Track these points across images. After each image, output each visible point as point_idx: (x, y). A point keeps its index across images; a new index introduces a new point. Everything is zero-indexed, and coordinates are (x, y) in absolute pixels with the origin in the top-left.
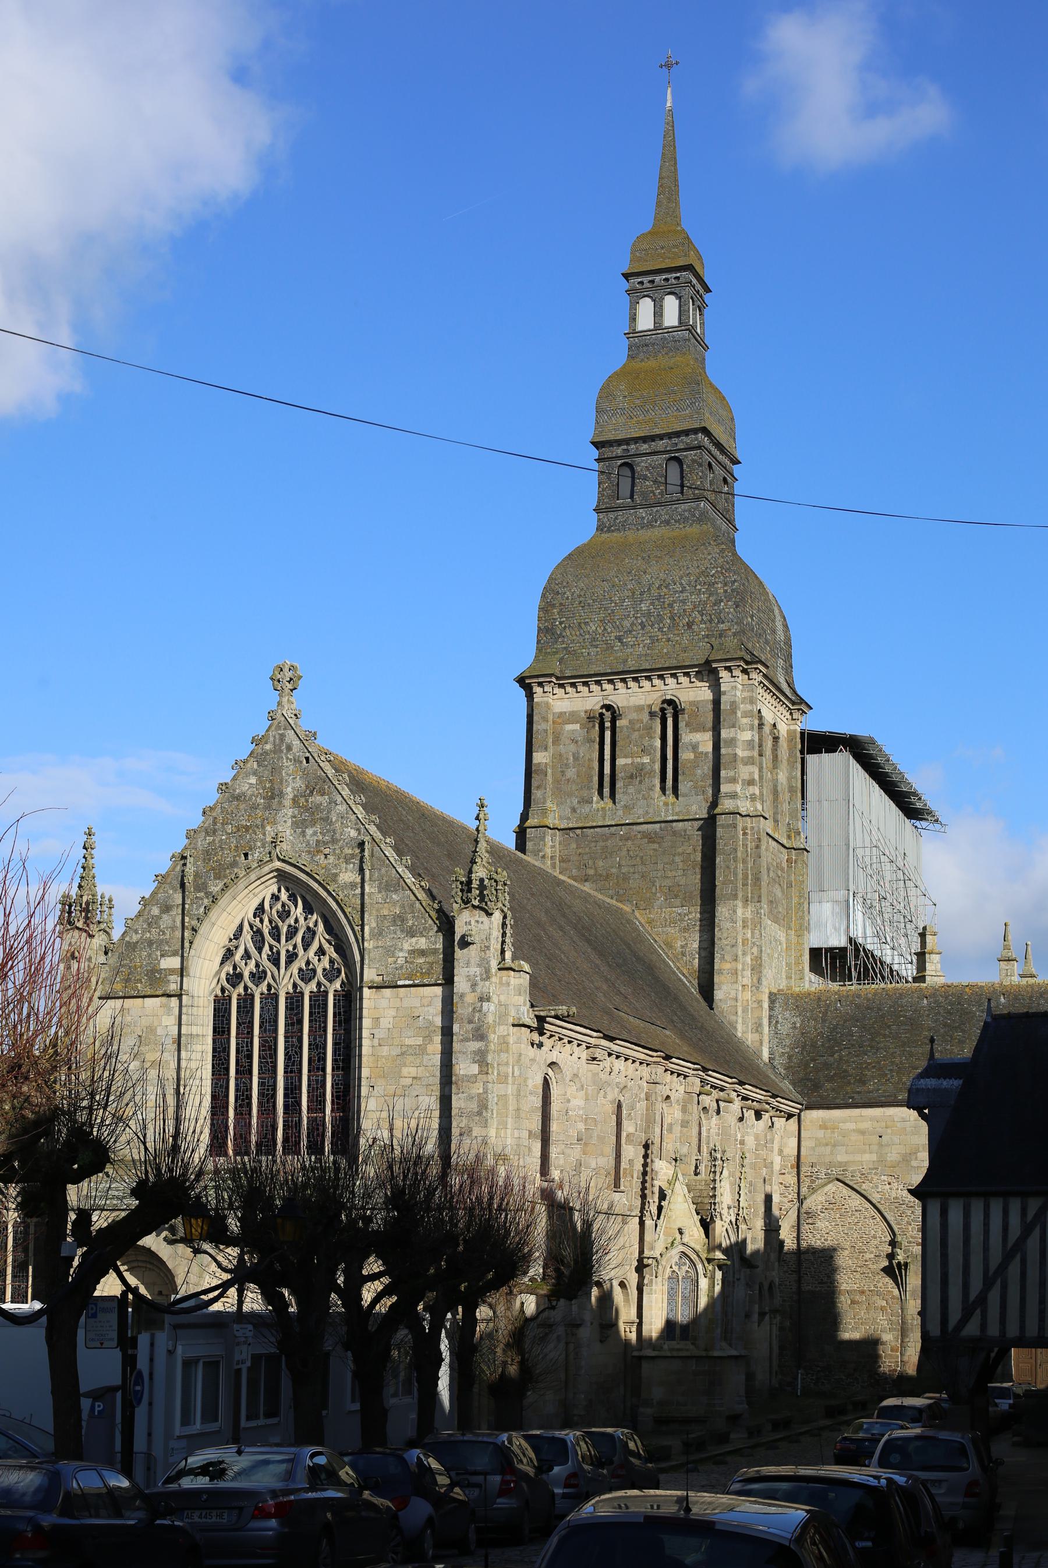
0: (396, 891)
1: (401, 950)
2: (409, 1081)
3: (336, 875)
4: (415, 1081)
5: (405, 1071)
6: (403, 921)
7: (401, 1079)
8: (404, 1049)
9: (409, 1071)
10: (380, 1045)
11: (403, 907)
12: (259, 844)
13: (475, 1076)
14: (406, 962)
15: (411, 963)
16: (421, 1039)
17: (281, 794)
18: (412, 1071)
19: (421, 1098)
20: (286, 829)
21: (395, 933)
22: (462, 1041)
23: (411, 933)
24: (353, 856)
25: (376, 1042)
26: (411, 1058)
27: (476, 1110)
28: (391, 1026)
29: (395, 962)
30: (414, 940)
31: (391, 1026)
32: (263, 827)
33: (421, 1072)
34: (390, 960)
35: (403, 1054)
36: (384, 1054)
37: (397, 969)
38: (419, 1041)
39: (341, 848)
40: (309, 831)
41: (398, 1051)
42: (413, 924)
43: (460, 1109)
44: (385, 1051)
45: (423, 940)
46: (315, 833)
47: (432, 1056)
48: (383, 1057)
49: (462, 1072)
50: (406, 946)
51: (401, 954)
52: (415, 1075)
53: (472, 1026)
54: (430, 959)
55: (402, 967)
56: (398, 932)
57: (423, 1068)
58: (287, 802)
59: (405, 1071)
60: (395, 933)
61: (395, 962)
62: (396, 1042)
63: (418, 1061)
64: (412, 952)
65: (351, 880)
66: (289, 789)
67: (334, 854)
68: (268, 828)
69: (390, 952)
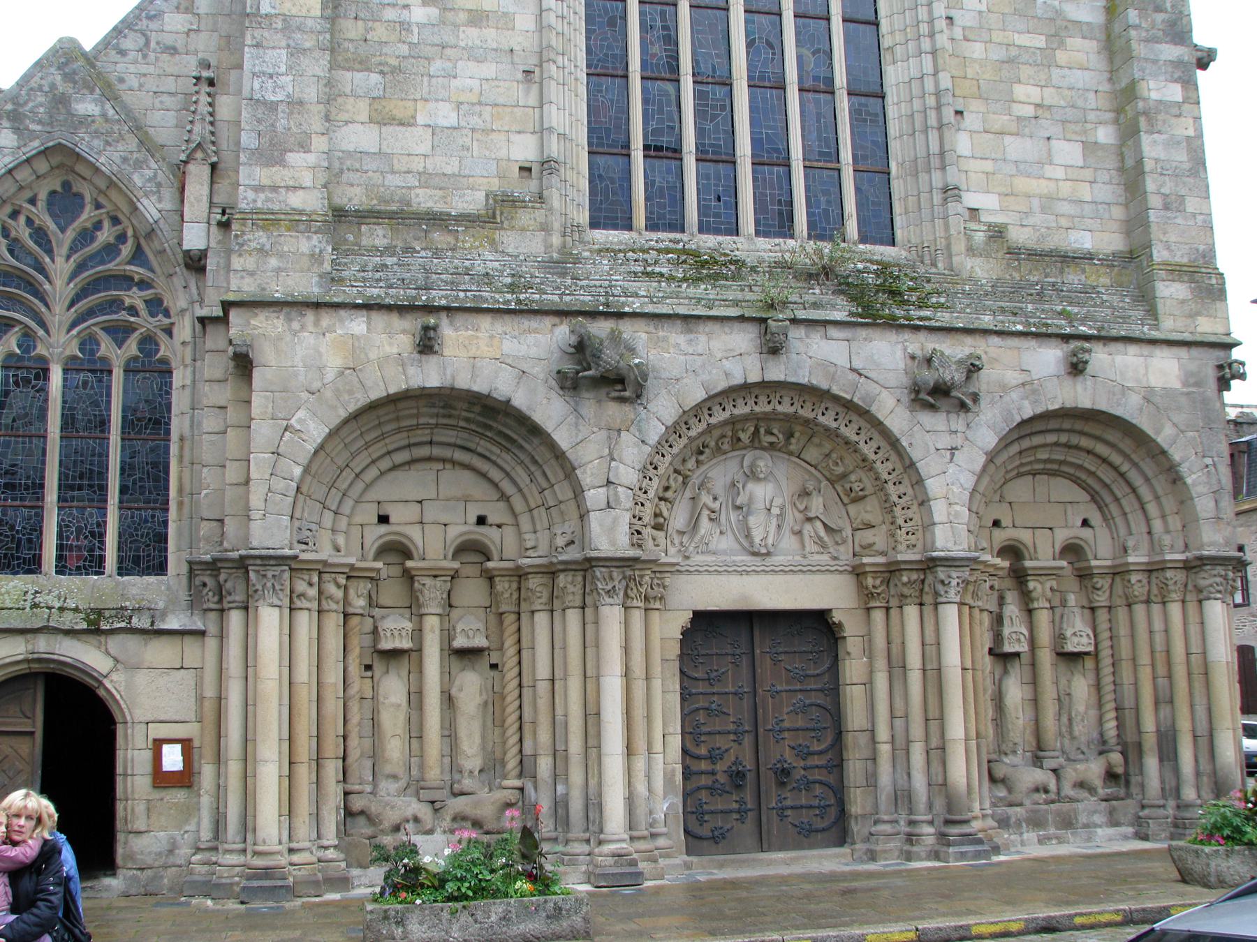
2: (1029, 111)
4: (1040, 112)
5: (1020, 91)
7: (1015, 106)
8: (1014, 52)
10: (966, 39)
16: (1043, 38)
18: (1034, 93)
19: (1053, 142)
22: (1147, 41)
25: (958, 32)
26: (1026, 71)
27: (1187, 166)
28: (984, 8)
31: (984, 8)
33: (1050, 96)
35: (1010, 61)
36: (975, 56)
41: (1000, 54)
43: (1157, 160)
44: (976, 50)
47: (1066, 71)
48: (975, 60)
52: (1038, 101)
57: (1052, 90)
59: (1020, 91)
62: (997, 36)
63: (1043, 76)
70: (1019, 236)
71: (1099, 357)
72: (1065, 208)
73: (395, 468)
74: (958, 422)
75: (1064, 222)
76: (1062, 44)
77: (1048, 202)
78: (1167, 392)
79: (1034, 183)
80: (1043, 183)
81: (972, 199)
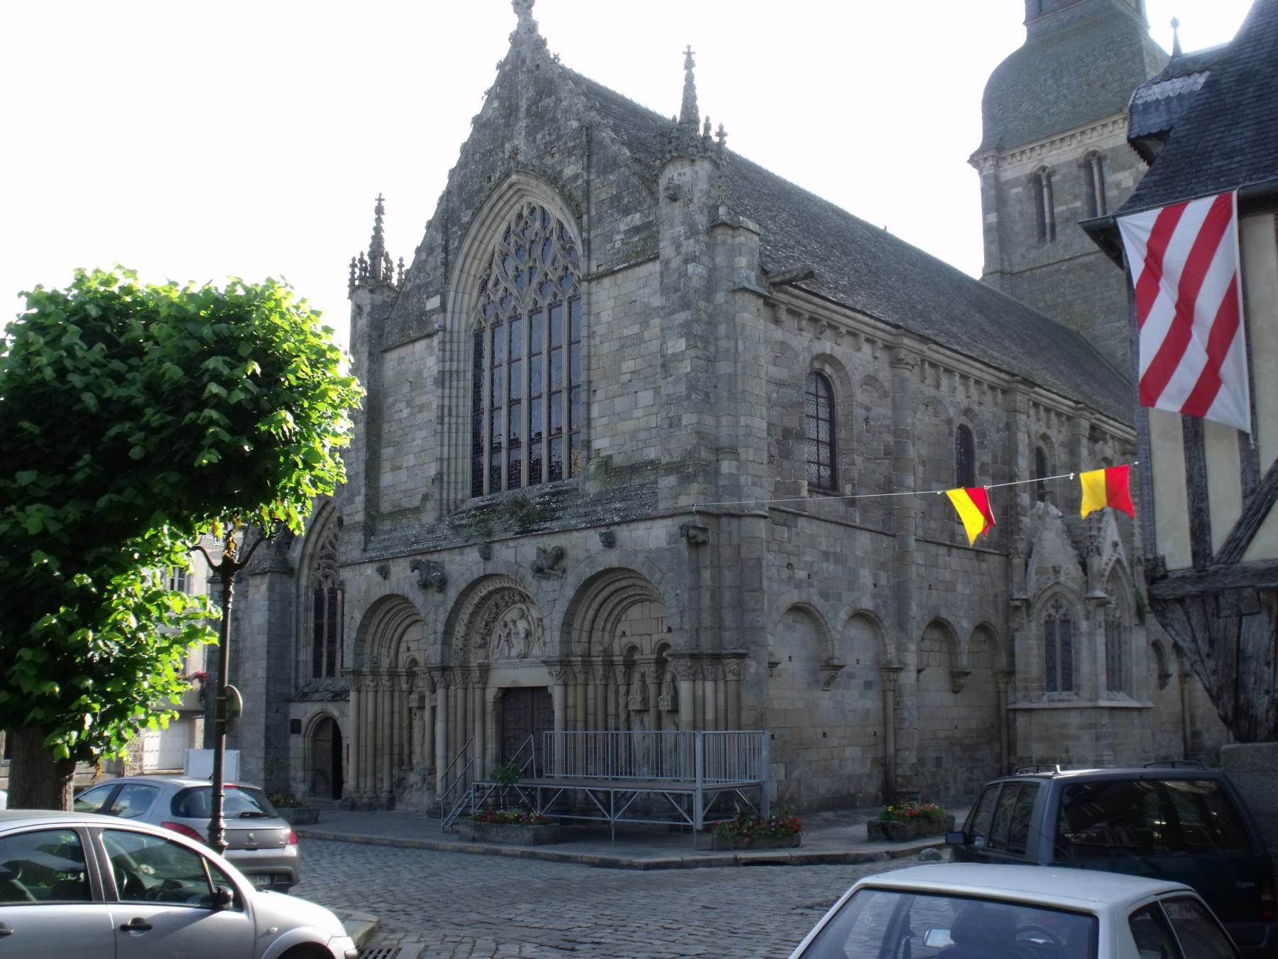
0: (612, 171)
1: (618, 233)
3: (561, 171)
6: (619, 201)
9: (628, 365)
11: (618, 186)
12: (500, 163)
13: (683, 352)
14: (623, 244)
15: (628, 244)
17: (517, 108)
19: (639, 394)
20: (520, 141)
21: (612, 216)
22: (669, 314)
23: (627, 212)
24: (574, 147)
27: (685, 393)
29: (613, 248)
30: (629, 218)
32: (503, 145)
33: (640, 363)
34: (609, 246)
35: (621, 348)
37: (614, 254)
38: (635, 329)
39: (565, 143)
40: (539, 136)
42: (629, 202)
45: (637, 216)
46: (544, 136)
49: (670, 352)
50: (623, 227)
51: (618, 237)
53: (679, 294)
54: (645, 234)
55: (619, 251)
56: (615, 214)
58: (522, 114)
60: (612, 216)
61: (613, 248)
64: (626, 232)
65: (573, 173)
66: (524, 101)
67: (559, 151)
68: (507, 145)
69: (608, 238)
70: (618, 460)
71: (623, 533)
72: (642, 435)
73: (409, 626)
74: (557, 585)
75: (640, 445)
76: (648, 325)
77: (633, 435)
78: (660, 550)
79: (627, 423)
80: (632, 421)
81: (597, 444)
